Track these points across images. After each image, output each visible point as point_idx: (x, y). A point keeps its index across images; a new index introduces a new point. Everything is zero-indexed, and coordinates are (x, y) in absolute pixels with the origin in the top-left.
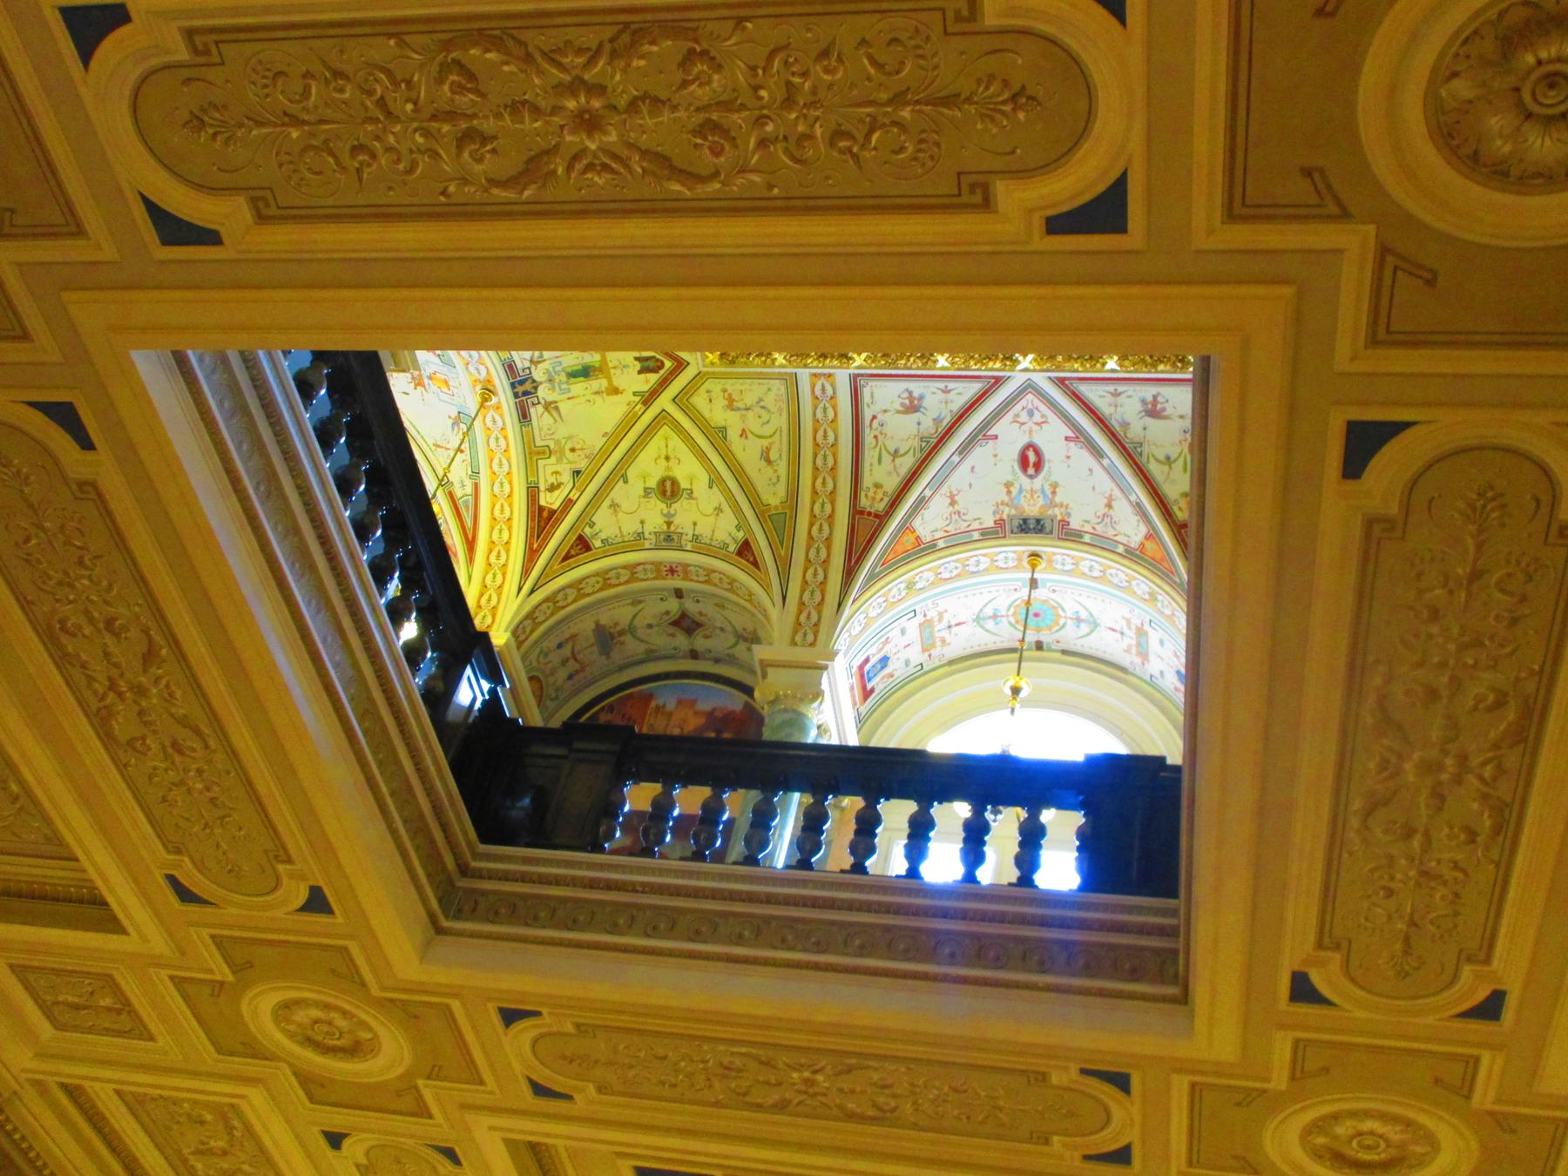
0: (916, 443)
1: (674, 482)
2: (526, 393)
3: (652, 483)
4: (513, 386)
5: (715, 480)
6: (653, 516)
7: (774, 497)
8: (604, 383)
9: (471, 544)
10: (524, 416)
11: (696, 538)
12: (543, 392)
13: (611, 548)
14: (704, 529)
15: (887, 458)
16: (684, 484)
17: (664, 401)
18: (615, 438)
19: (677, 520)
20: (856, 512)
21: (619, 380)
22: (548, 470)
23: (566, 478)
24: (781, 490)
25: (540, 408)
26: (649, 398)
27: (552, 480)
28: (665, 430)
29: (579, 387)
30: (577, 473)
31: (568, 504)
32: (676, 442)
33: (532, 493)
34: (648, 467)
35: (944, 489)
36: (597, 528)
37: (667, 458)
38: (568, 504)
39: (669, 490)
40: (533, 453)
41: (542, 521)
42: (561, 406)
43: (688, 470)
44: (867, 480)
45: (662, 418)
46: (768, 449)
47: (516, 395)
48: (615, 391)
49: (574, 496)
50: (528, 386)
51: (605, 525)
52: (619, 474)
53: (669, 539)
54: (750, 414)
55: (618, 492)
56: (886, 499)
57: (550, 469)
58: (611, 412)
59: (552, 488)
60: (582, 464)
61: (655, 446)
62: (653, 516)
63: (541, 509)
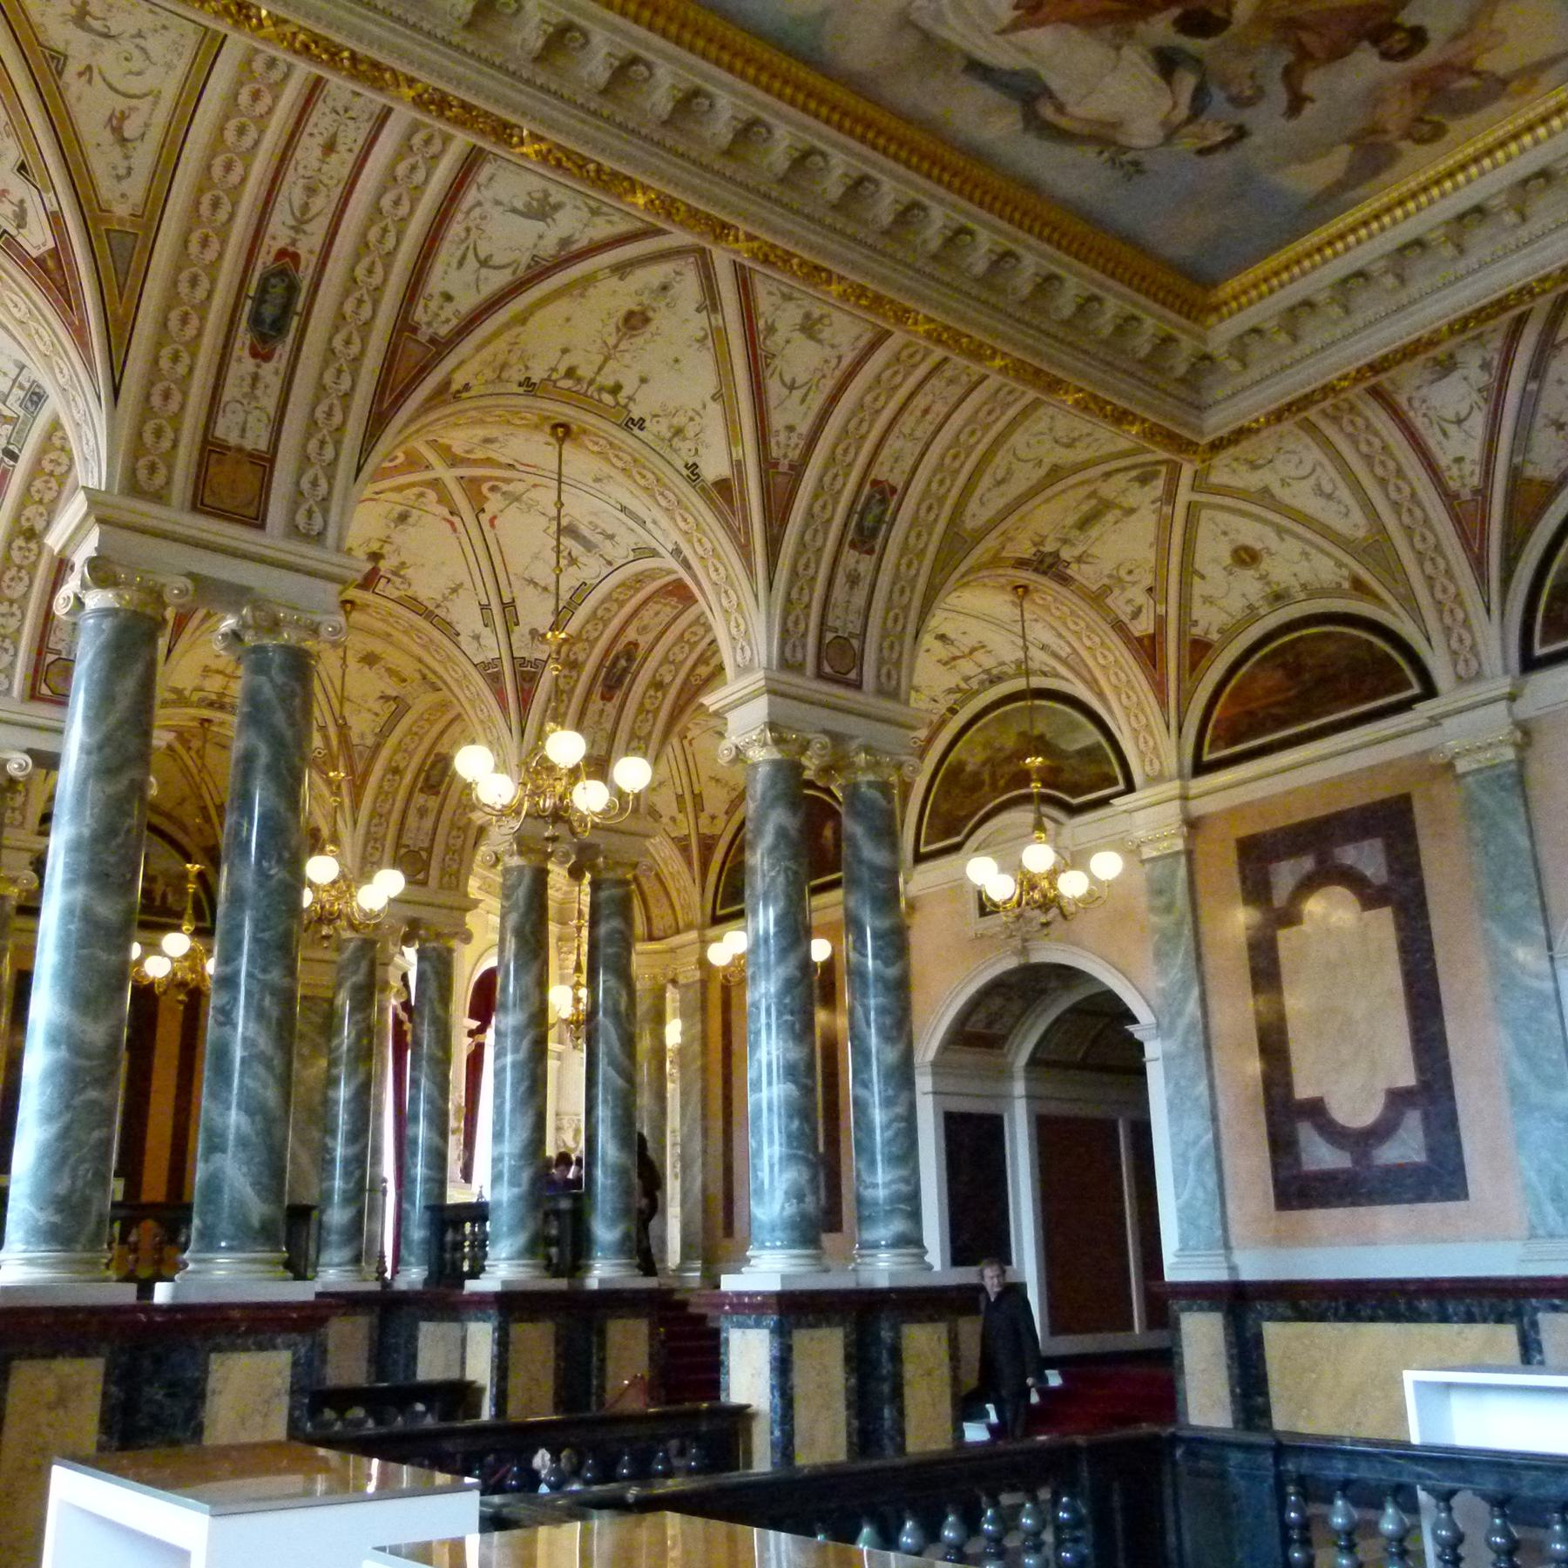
0: (1475, 396)
1: (1246, 549)
2: (1051, 566)
3: (1228, 560)
4: (1036, 570)
5: (1281, 531)
6: (1248, 586)
7: (1354, 524)
8: (1117, 512)
9: (1101, 695)
10: (1065, 580)
11: (1304, 587)
12: (1066, 554)
13: (1229, 634)
14: (1306, 575)
15: (1452, 429)
16: (1258, 546)
17: (1184, 495)
18: (1162, 544)
19: (1274, 577)
20: (1449, 498)
21: (1130, 502)
22: (1119, 604)
23: (1141, 598)
24: (1357, 516)
25: (1074, 566)
26: (1170, 496)
27: (1129, 609)
28: (1205, 514)
29: (1094, 532)
30: (1150, 590)
31: (1161, 621)
32: (1223, 517)
33: (1119, 627)
34: (1212, 551)
35: (1539, 422)
36: (1203, 624)
37: (1225, 533)
38: (1161, 621)
39: (1246, 557)
40: (1097, 599)
41: (1148, 650)
42: (1094, 551)
43: (1249, 533)
44: (1444, 460)
45: (1192, 509)
46: (1319, 486)
47: (1045, 573)
48: (1131, 511)
49: (1161, 609)
50: (1049, 560)
51: (1208, 621)
52: (1188, 570)
53: (1279, 598)
54: (1278, 464)
55: (1199, 588)
56: (1477, 470)
57: (1121, 602)
58: (1143, 527)
59: (1136, 614)
60: (1148, 580)
61: (1205, 530)
62: (1248, 586)
63: (1140, 640)
